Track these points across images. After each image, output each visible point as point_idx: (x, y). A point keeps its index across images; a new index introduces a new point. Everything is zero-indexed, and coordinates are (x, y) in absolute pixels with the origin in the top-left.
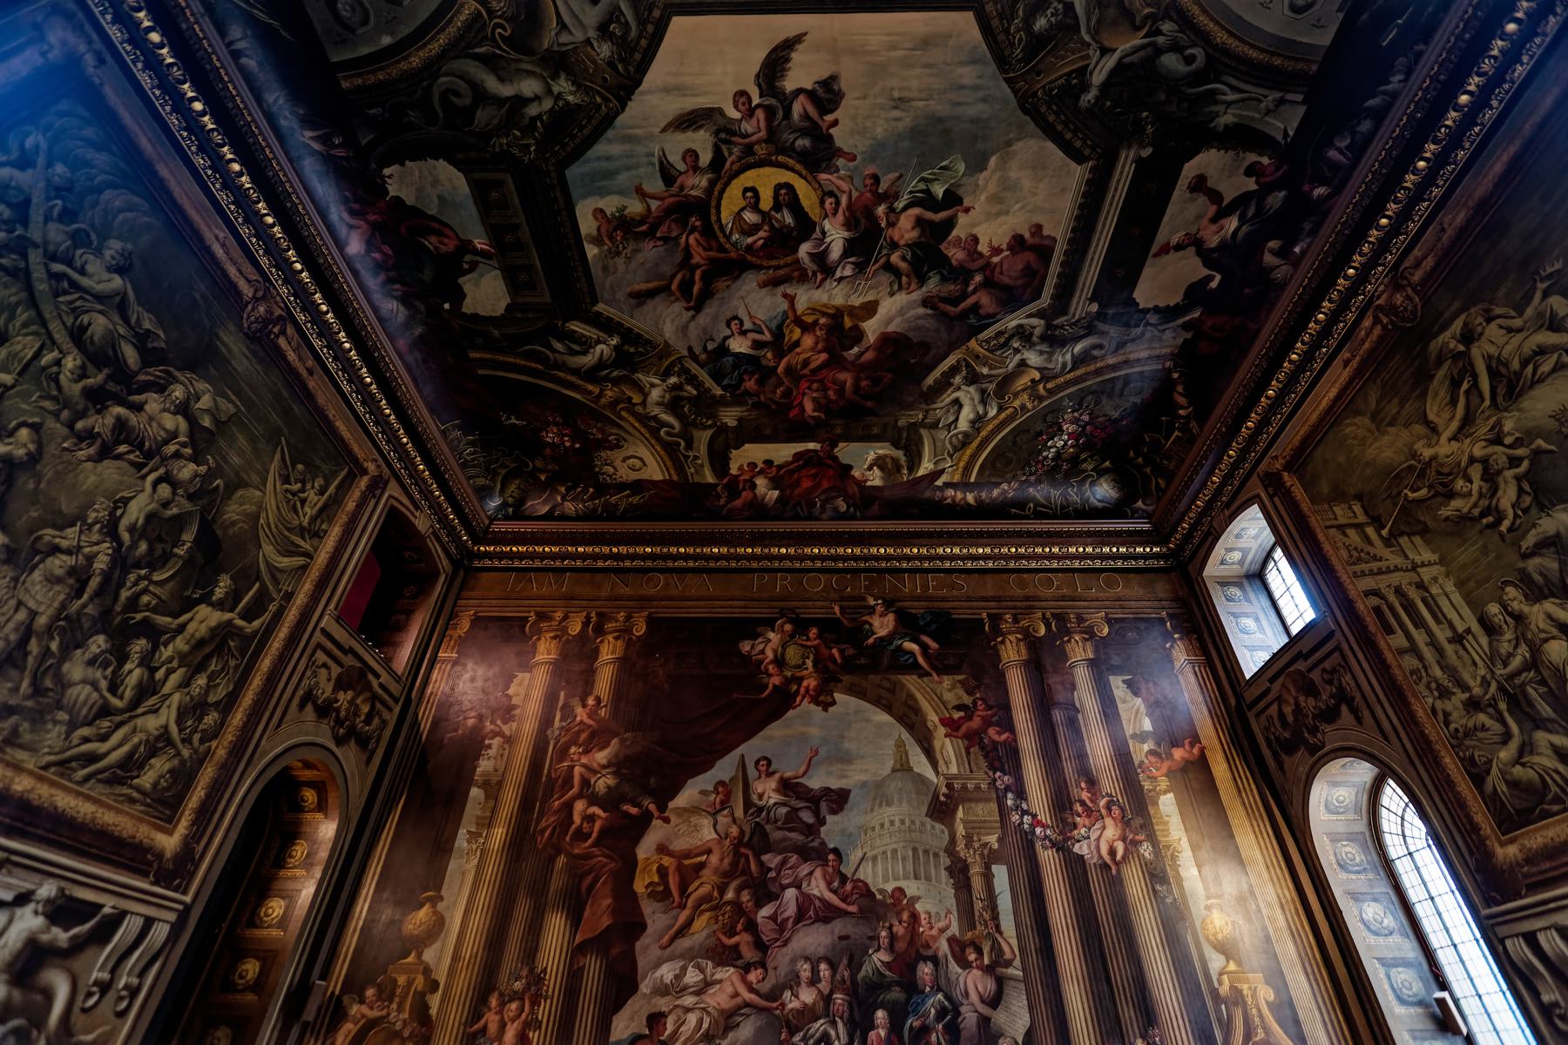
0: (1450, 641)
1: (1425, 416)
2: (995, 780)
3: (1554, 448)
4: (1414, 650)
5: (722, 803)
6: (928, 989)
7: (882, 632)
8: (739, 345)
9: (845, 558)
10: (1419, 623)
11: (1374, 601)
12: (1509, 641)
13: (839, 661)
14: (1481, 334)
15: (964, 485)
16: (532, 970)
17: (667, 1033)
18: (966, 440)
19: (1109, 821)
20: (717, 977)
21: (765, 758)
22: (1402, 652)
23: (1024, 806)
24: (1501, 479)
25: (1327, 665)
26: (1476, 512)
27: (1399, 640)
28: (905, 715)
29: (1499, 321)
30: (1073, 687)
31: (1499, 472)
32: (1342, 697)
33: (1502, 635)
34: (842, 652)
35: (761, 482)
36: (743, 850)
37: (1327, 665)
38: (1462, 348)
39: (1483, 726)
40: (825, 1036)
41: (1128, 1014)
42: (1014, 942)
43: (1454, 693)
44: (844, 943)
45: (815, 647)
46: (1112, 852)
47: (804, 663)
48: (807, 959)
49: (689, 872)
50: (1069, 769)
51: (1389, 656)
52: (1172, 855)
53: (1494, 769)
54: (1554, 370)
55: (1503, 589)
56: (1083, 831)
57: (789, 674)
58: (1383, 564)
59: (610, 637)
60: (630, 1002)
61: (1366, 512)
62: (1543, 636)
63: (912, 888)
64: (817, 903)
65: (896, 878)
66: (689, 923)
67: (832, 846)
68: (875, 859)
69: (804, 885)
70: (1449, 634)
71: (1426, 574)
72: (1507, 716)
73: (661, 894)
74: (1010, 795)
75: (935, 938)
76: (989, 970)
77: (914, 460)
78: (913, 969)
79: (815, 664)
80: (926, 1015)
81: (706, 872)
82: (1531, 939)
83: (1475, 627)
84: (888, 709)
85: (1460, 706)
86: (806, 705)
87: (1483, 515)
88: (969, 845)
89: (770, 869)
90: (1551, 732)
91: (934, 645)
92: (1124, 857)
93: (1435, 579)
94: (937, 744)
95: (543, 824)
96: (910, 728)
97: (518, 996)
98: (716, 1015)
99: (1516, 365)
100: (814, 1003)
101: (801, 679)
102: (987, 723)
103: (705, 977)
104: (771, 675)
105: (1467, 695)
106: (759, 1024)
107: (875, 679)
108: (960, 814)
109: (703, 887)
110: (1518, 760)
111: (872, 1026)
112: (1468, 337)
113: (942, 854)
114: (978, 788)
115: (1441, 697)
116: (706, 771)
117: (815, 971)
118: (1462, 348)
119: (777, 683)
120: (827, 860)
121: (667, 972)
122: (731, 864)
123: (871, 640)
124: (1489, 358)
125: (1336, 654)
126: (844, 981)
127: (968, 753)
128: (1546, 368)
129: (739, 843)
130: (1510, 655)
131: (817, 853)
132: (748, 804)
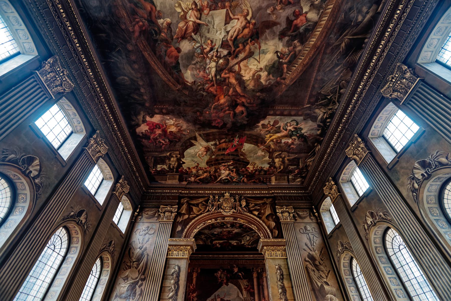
7: (236, 271)
8: (215, 233)
9: (231, 257)
15: (249, 245)
18: (248, 240)
30: (263, 282)
35: (218, 245)
50: (261, 296)
59: (195, 273)
77: (241, 242)
86: (224, 285)
91: (243, 274)
94: (243, 292)
96: (239, 289)
101: (224, 280)
102: (251, 288)
114: (248, 300)
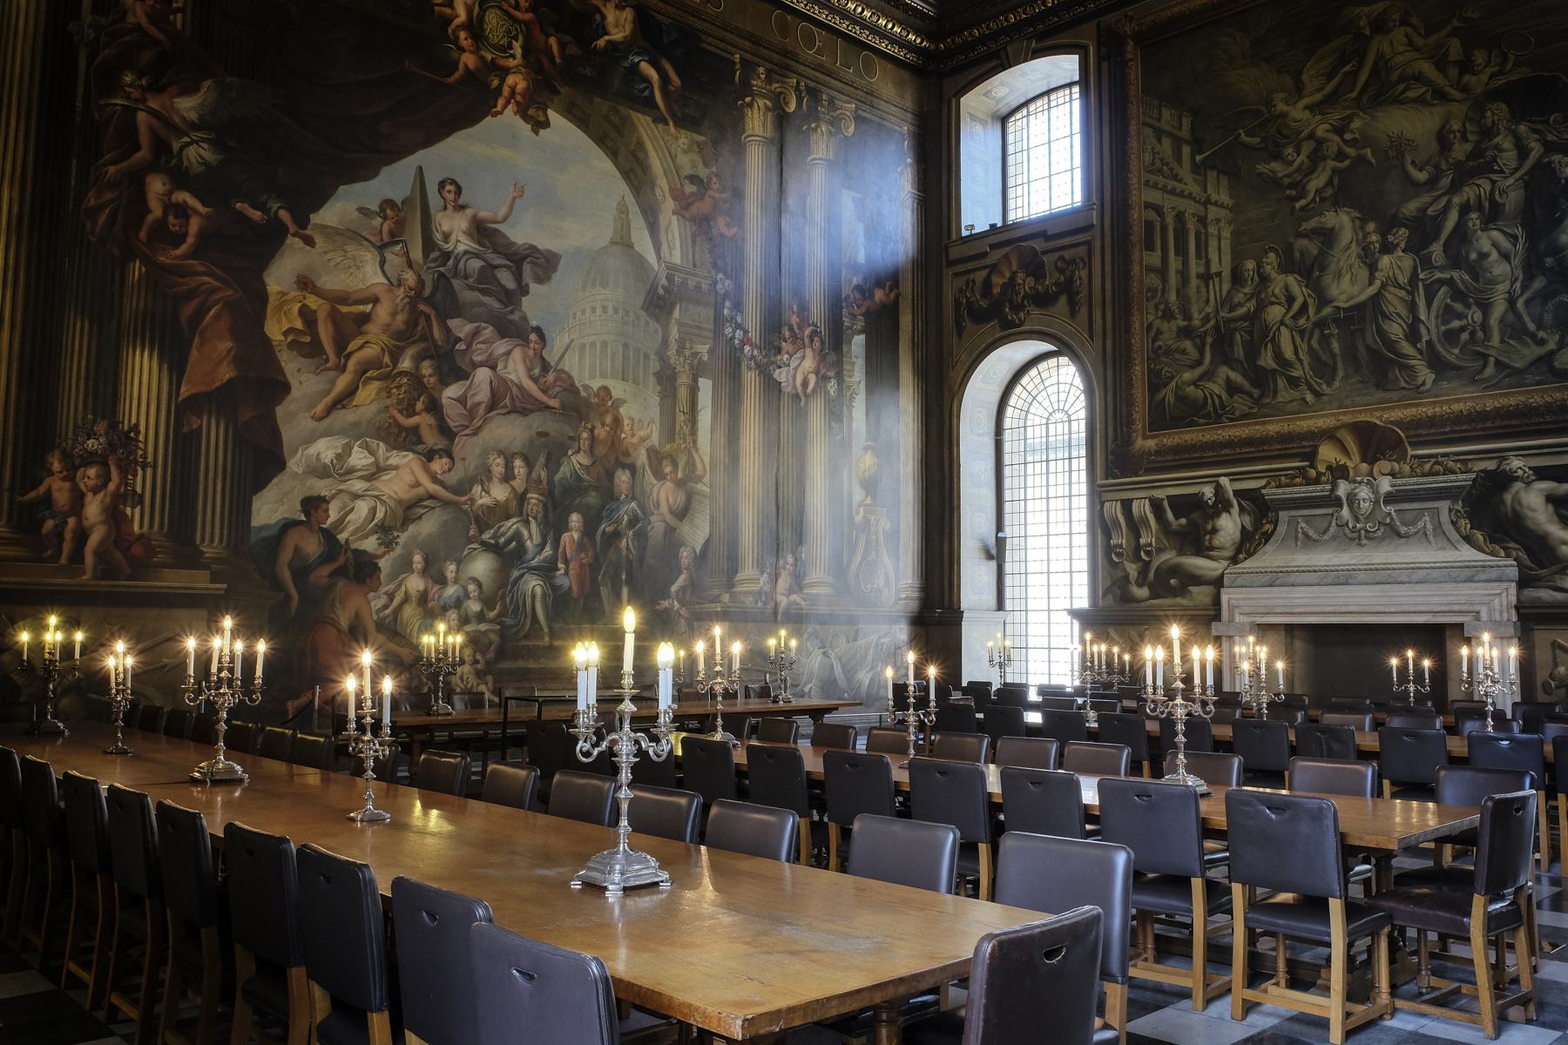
0: (1199, 276)
1: (1301, 73)
2: (715, 282)
3: (1374, 161)
4: (1163, 272)
5: (392, 234)
6: (623, 496)
7: (617, 35)
10: (1181, 250)
11: (1153, 215)
12: (1246, 294)
13: (558, 60)
14: (1390, 31)
16: (114, 425)
17: (329, 521)
19: (809, 352)
20: (390, 462)
21: (453, 182)
22: (1150, 269)
23: (739, 320)
24: (1322, 164)
25: (1067, 254)
26: (1287, 181)
27: (1154, 259)
28: (632, 170)
29: (1409, 30)
31: (1325, 158)
32: (1068, 288)
33: (1243, 287)
34: (562, 45)
36: (422, 307)
37: (1067, 254)
38: (1367, 32)
39: (1185, 350)
40: (517, 536)
41: (787, 534)
42: (707, 459)
43: (1176, 319)
44: (544, 439)
45: (527, 23)
46: (805, 384)
47: (510, 46)
48: (500, 453)
49: (350, 326)
51: (1136, 269)
52: (851, 395)
53: (1173, 383)
54: (1415, 100)
55: (1267, 253)
56: (786, 356)
57: (489, 57)
58: (1180, 186)
60: (275, 481)
61: (1193, 129)
62: (1273, 299)
63: (618, 389)
64: (514, 390)
65: (604, 376)
66: (351, 392)
67: (534, 323)
68: (582, 347)
69: (500, 367)
70: (1201, 270)
71: (1213, 213)
72: (1208, 348)
73: (312, 350)
74: (727, 304)
75: (636, 446)
76: (680, 484)
78: (610, 475)
79: (524, 56)
80: (618, 522)
81: (372, 328)
82: (1127, 505)
83: (1226, 273)
84: (613, 154)
85: (1175, 329)
87: (1290, 186)
88: (680, 352)
89: (459, 340)
90: (1233, 369)
92: (814, 391)
93: (1218, 220)
95: (92, 201)
97: (90, 459)
98: (392, 504)
99: (1395, 76)
100: (507, 501)
101: (504, 72)
103: (377, 461)
104: (462, 50)
105: (1186, 323)
106: (445, 518)
107: (602, 105)
108: (676, 314)
109: (369, 346)
110: (1195, 383)
111: (566, 529)
112: (1379, 26)
113: (653, 357)
114: (698, 287)
115: (1162, 318)
116: (366, 179)
117: (509, 467)
118: (1367, 32)
119: (471, 66)
120: (527, 341)
121: (325, 449)
122: (406, 323)
123: (601, 42)
124: (1380, 56)
125: (1082, 250)
126: (539, 481)
127: (694, 242)
128: (1411, 94)
129: (416, 296)
130: (1240, 305)
131: (513, 330)
132: (429, 244)
